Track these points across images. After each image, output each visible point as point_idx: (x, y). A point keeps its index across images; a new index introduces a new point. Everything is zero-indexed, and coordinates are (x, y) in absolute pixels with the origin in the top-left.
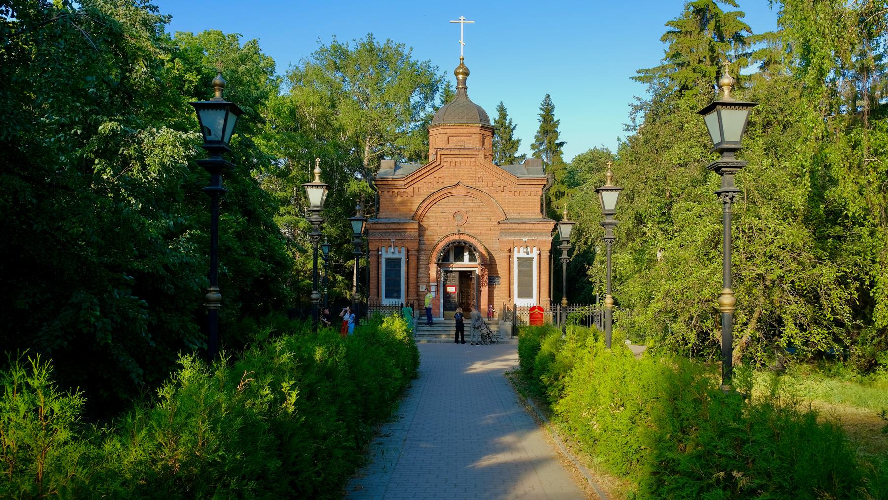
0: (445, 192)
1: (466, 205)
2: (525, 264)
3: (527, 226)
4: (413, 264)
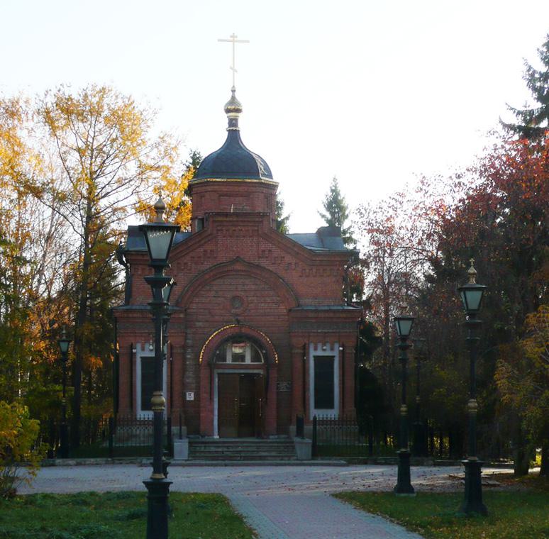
0: (221, 271)
2: (324, 364)
4: (178, 366)
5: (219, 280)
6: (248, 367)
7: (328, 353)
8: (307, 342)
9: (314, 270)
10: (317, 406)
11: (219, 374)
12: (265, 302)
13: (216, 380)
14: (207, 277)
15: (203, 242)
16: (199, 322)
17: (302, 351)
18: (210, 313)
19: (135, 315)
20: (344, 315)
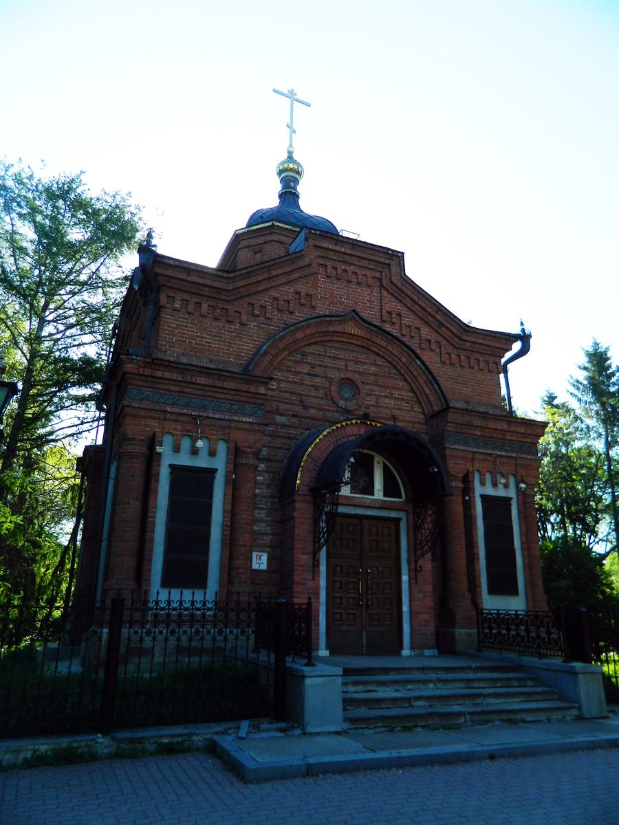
1: (360, 368)
5: (316, 347)
8: (471, 469)
12: (391, 396)
14: (300, 335)
15: (295, 276)
16: (282, 415)
17: (461, 485)
18: (301, 401)
20: (522, 430)
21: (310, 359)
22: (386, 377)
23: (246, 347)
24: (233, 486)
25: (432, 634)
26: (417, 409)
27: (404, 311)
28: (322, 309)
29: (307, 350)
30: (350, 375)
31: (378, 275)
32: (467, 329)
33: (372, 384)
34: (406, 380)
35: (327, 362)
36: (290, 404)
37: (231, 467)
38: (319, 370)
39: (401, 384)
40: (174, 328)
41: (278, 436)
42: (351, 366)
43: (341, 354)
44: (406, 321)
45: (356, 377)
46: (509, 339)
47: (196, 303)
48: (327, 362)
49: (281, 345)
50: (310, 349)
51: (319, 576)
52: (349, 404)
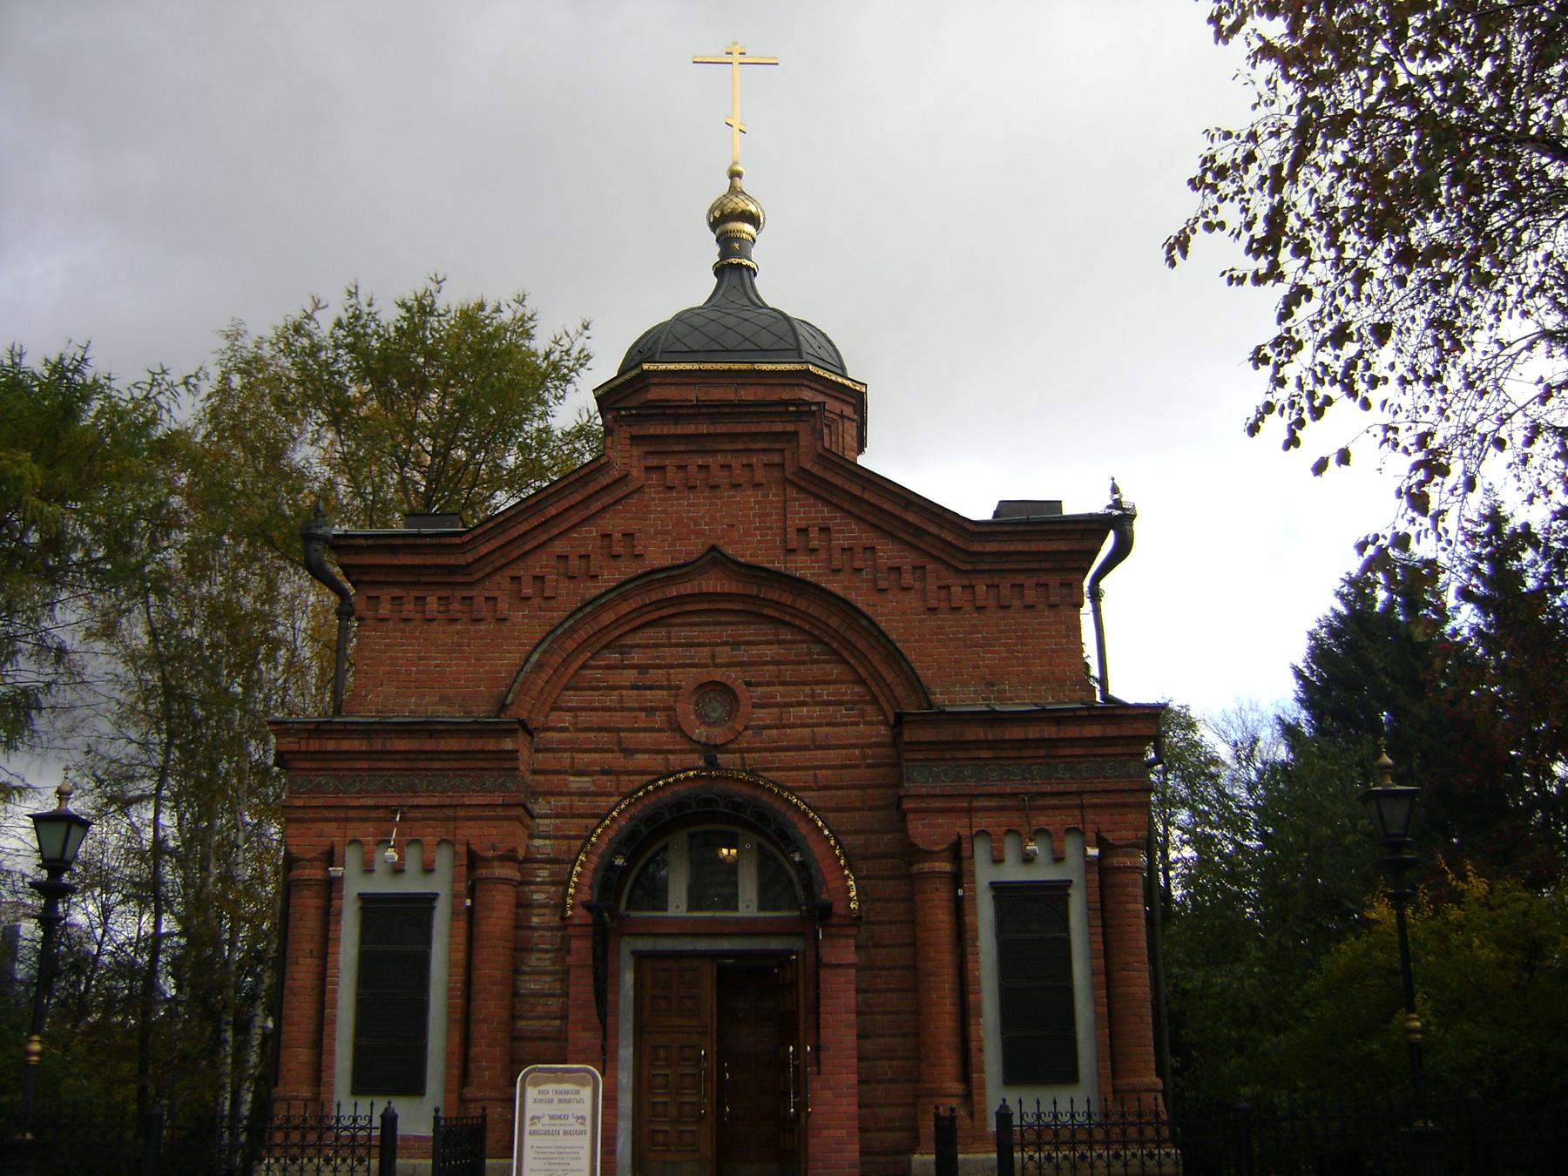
1: (744, 654)
3: (1032, 732)
5: (651, 632)
6: (748, 929)
7: (1043, 872)
8: (964, 832)
9: (981, 589)
10: (1015, 1074)
11: (639, 956)
13: (628, 978)
14: (608, 617)
16: (580, 773)
17: (946, 867)
19: (346, 745)
21: (636, 657)
22: (804, 663)
23: (507, 659)
24: (470, 920)
25: (851, 1166)
26: (871, 713)
27: (837, 520)
28: (657, 555)
29: (628, 641)
30: (718, 675)
31: (776, 459)
32: (976, 529)
33: (769, 684)
34: (845, 661)
35: (670, 655)
36: (596, 750)
37: (462, 887)
38: (657, 675)
39: (835, 670)
40: (380, 651)
41: (573, 816)
42: (724, 653)
43: (696, 634)
44: (840, 541)
45: (733, 676)
46: (1093, 527)
47: (417, 598)
48: (670, 655)
49: (570, 645)
50: (638, 639)
51: (616, 1068)
52: (716, 731)
